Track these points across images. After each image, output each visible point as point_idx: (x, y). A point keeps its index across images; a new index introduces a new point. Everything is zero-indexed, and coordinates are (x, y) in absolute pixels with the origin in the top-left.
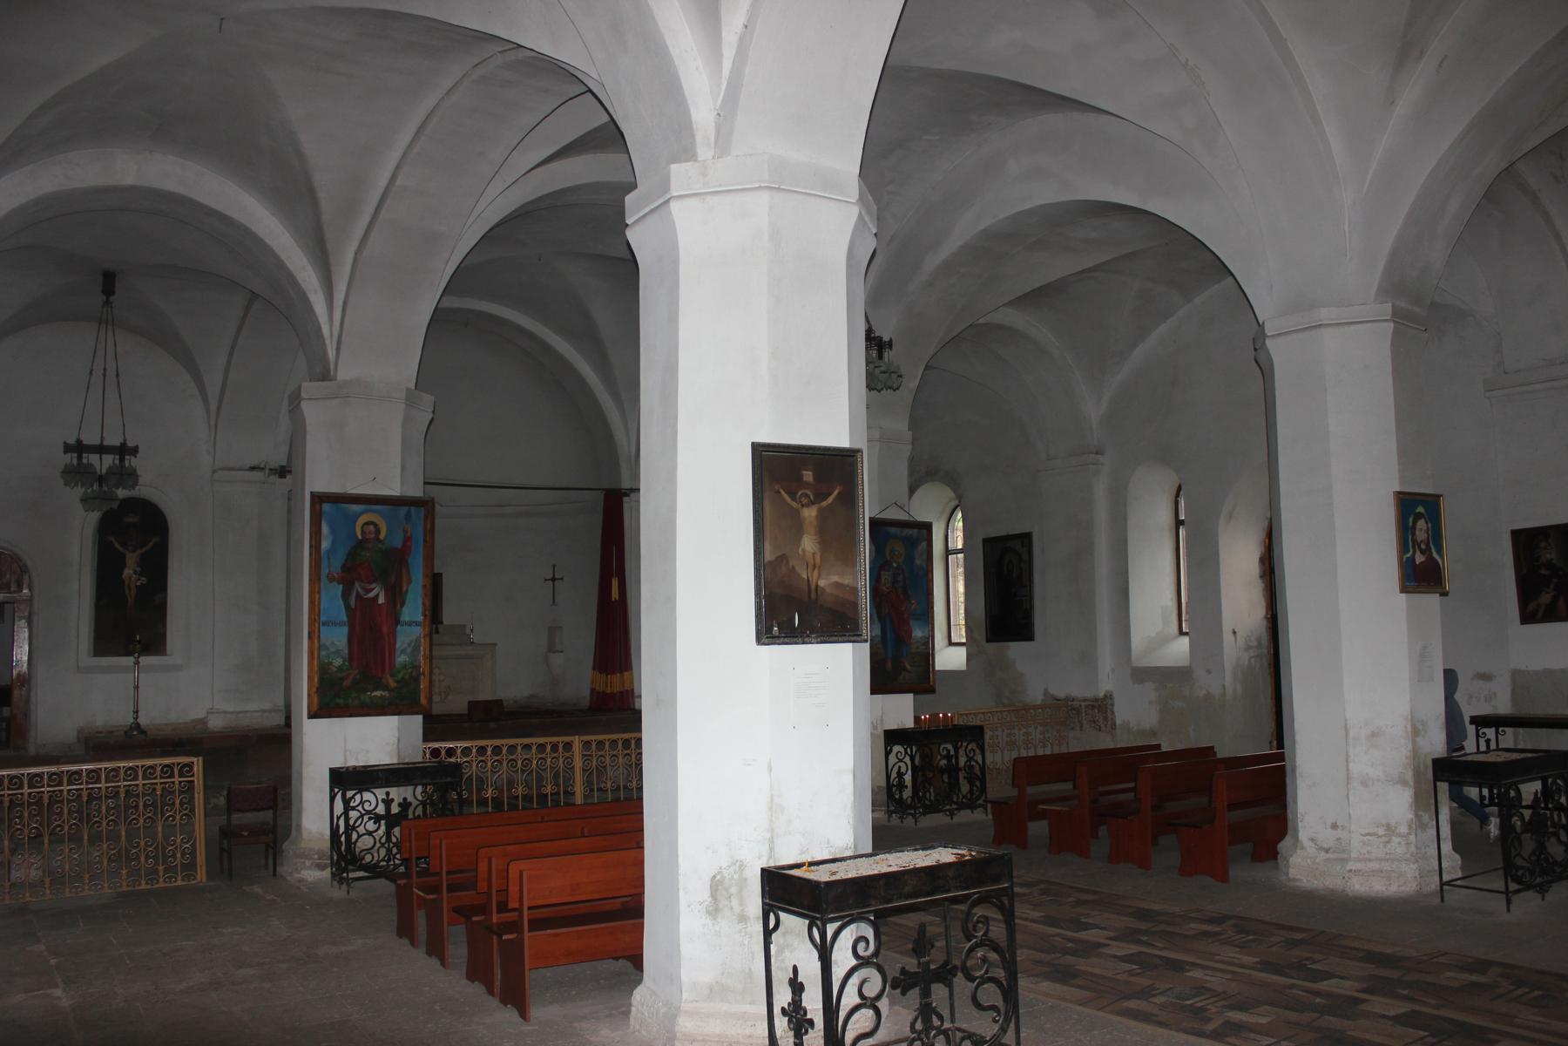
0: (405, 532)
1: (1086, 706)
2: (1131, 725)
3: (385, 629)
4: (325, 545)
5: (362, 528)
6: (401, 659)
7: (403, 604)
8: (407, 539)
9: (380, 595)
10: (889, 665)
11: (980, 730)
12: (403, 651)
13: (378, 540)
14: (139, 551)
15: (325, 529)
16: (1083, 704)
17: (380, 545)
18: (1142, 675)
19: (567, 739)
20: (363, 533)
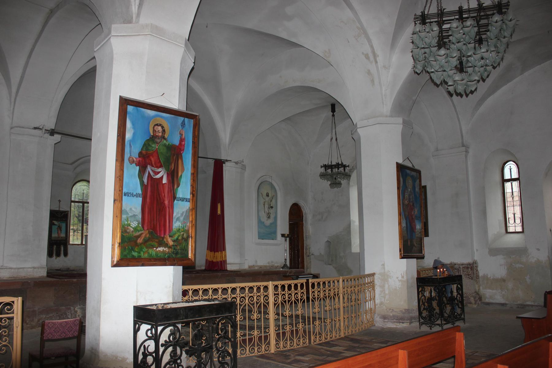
0: (181, 135)
1: (463, 268)
2: (489, 277)
3: (166, 202)
4: (129, 136)
5: (154, 128)
6: (176, 225)
7: (178, 186)
8: (182, 140)
9: (164, 176)
11: (460, 277)
12: (178, 219)
13: (164, 138)
15: (129, 124)
16: (461, 266)
17: (165, 142)
18: (494, 252)
19: (265, 284)
20: (154, 131)
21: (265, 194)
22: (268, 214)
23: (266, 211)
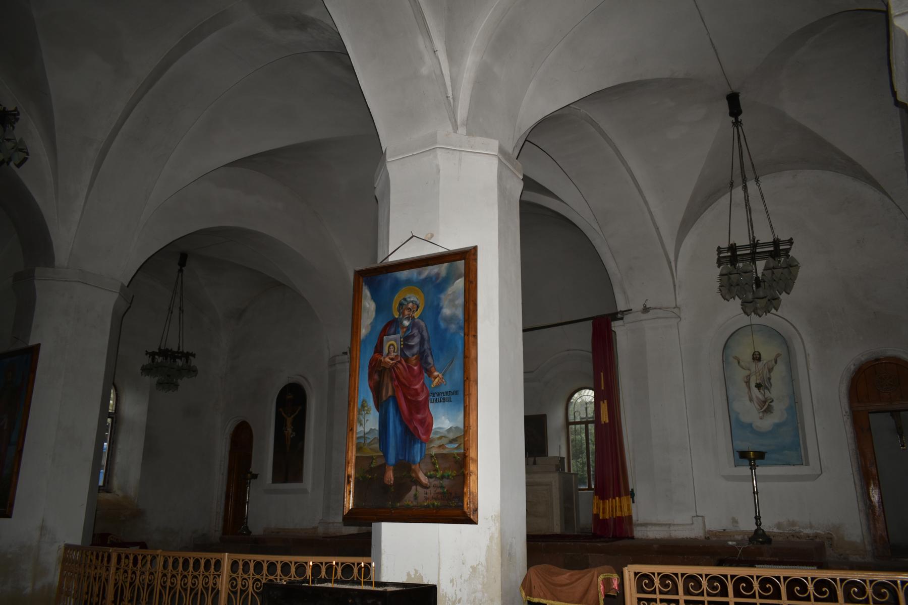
10: (390, 476)
14: (292, 416)
21: (746, 356)
22: (765, 402)
23: (757, 397)
